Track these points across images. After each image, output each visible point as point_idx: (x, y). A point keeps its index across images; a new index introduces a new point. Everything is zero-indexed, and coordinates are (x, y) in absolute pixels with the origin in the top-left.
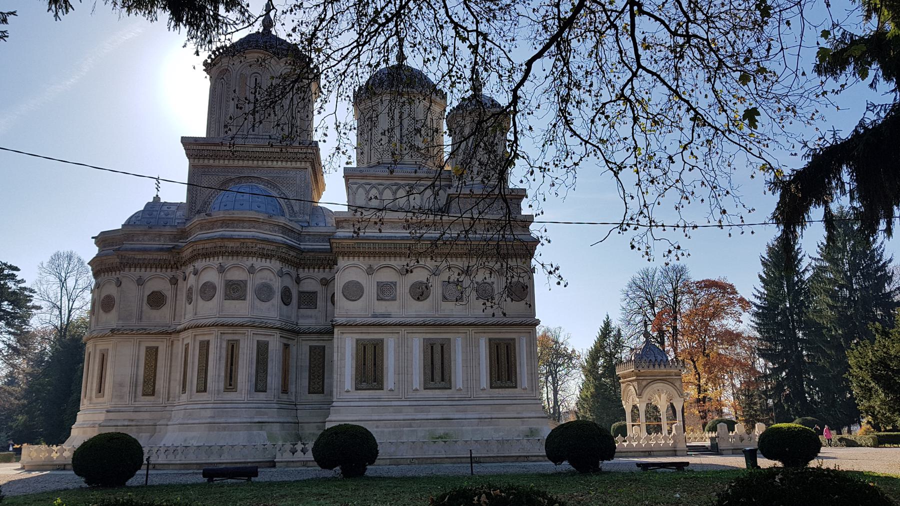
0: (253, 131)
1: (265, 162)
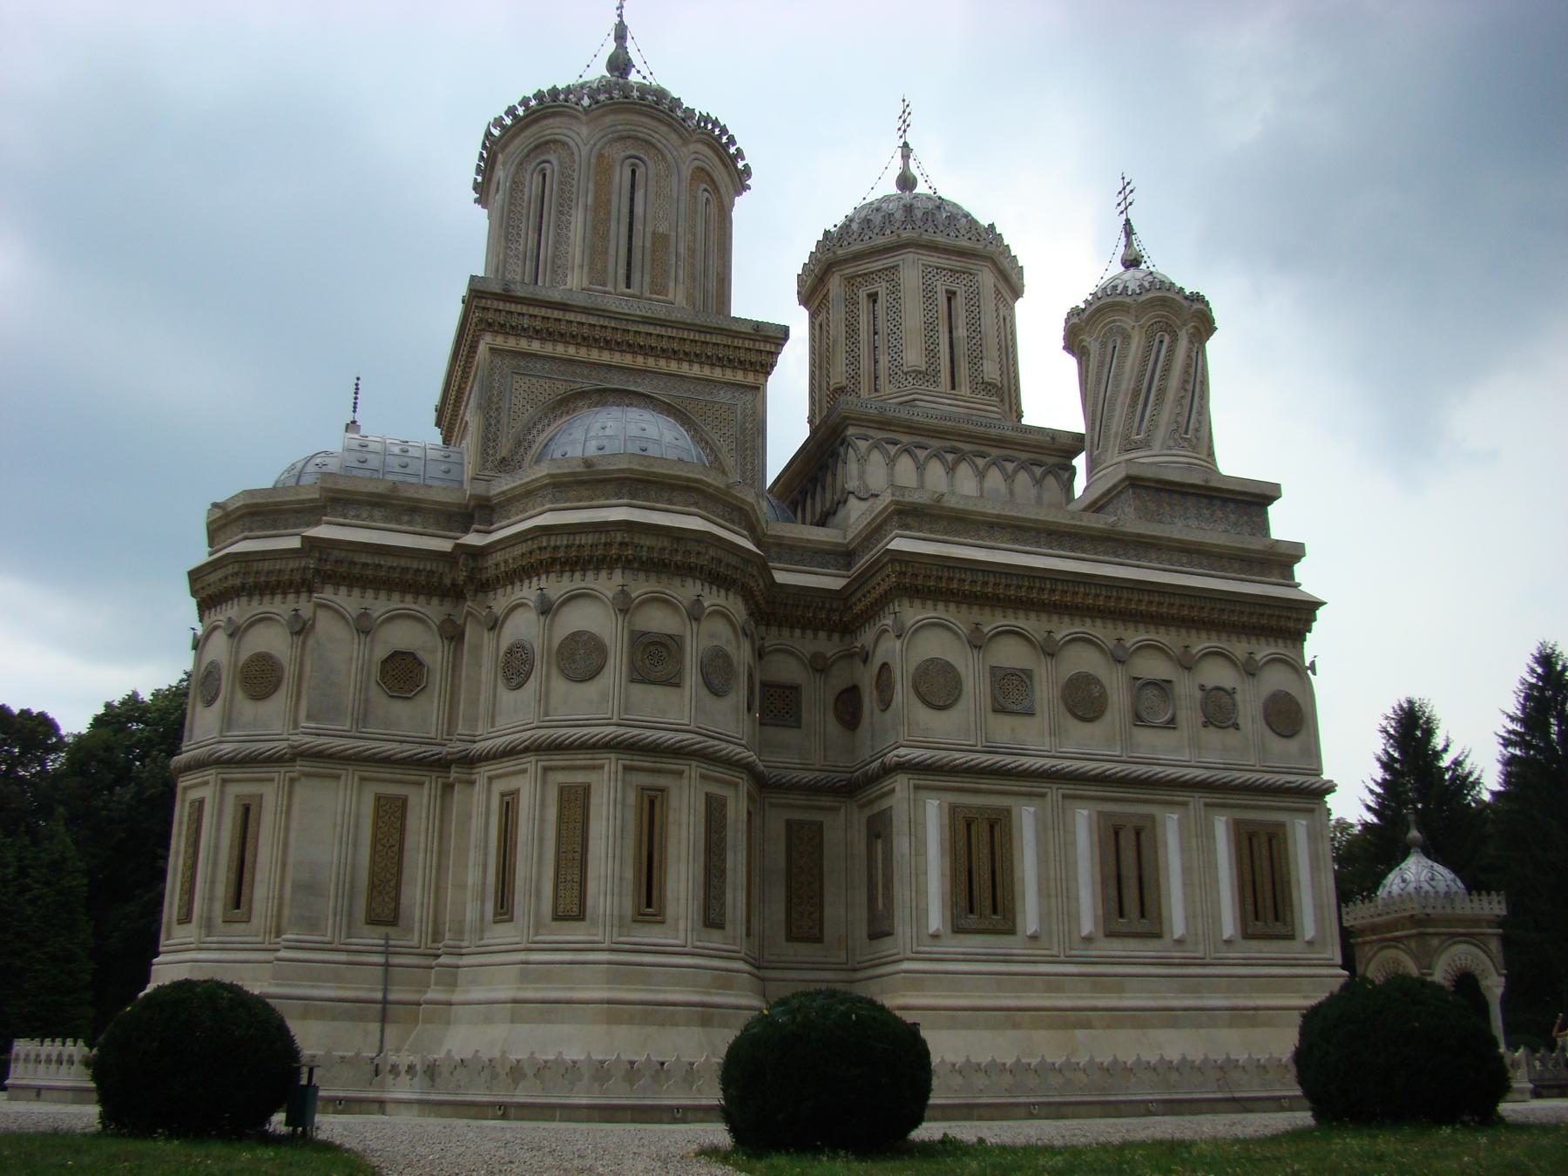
0: (628, 286)
1: (662, 363)
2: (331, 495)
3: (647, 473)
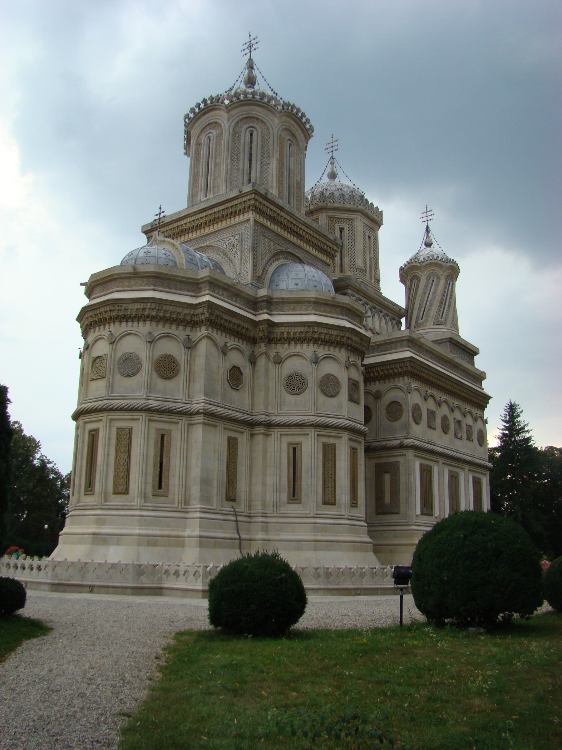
2: (211, 280)
3: (352, 307)
